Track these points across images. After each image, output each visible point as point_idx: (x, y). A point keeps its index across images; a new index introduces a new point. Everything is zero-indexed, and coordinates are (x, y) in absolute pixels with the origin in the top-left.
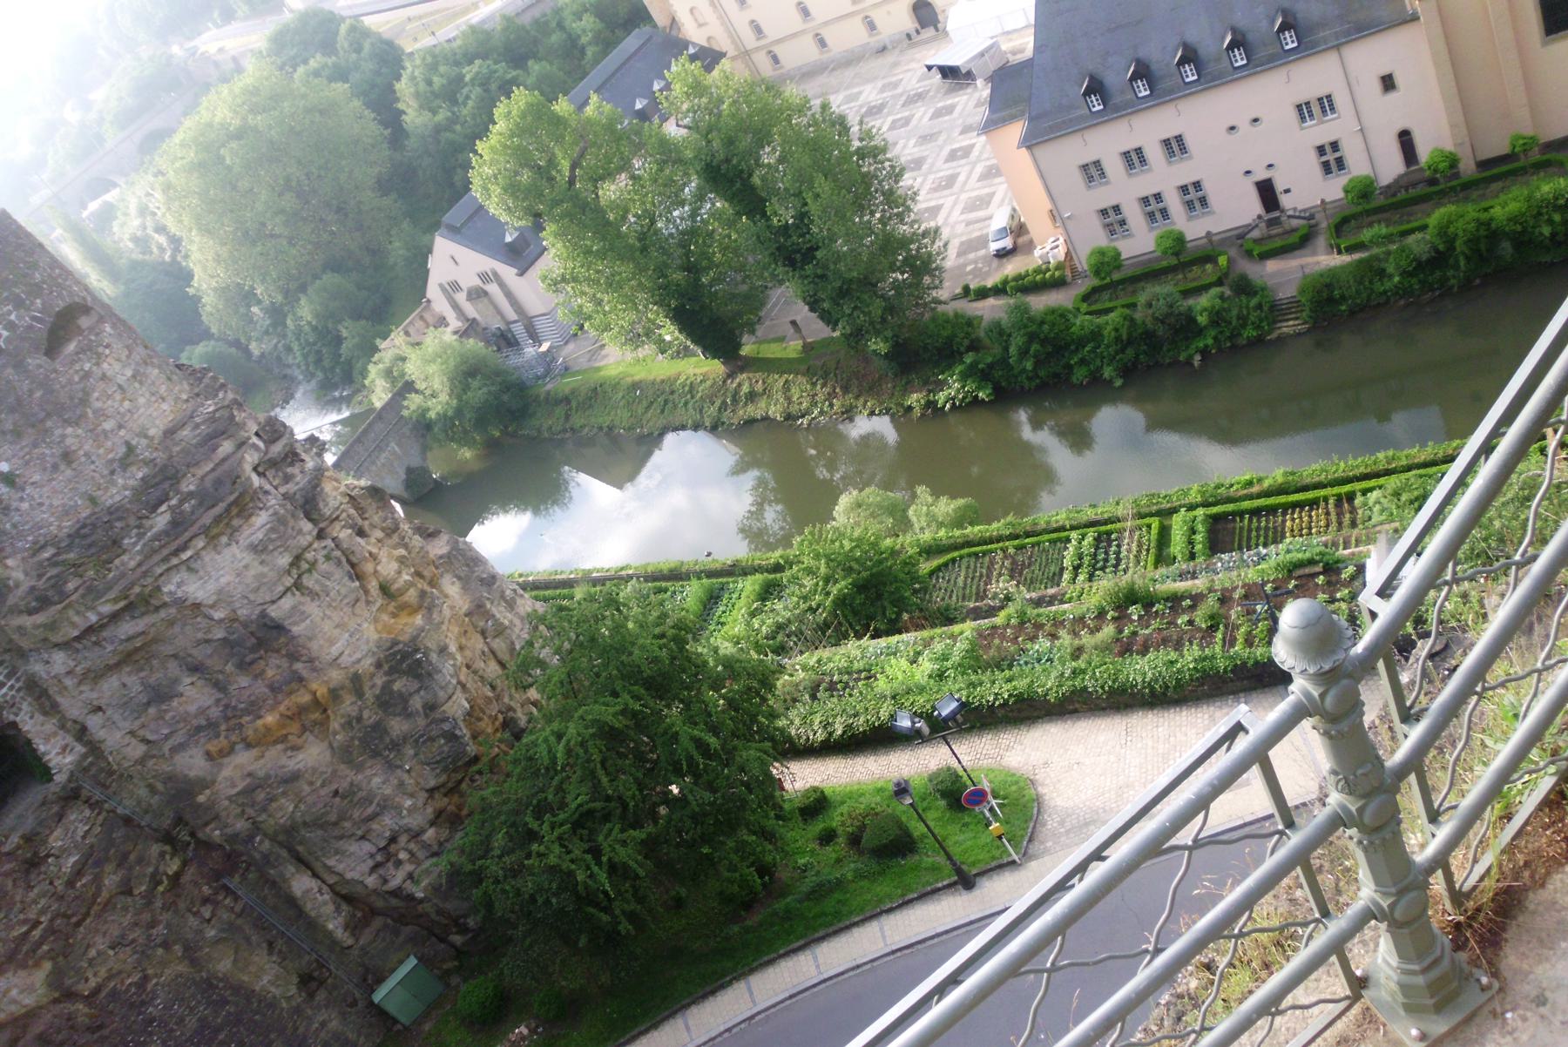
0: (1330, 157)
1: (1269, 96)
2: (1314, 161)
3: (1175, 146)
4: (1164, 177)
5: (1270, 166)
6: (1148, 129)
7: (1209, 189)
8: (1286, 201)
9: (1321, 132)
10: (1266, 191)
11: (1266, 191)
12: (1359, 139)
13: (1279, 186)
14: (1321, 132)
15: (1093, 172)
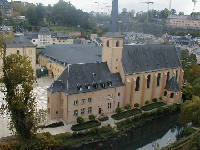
0: (110, 105)
1: (104, 93)
2: (107, 105)
3: (90, 100)
4: (86, 105)
5: (102, 106)
6: (86, 96)
7: (93, 108)
8: (102, 112)
9: (109, 100)
10: (100, 110)
11: (100, 110)
12: (113, 103)
13: (102, 110)
14: (109, 100)
15: (76, 102)
